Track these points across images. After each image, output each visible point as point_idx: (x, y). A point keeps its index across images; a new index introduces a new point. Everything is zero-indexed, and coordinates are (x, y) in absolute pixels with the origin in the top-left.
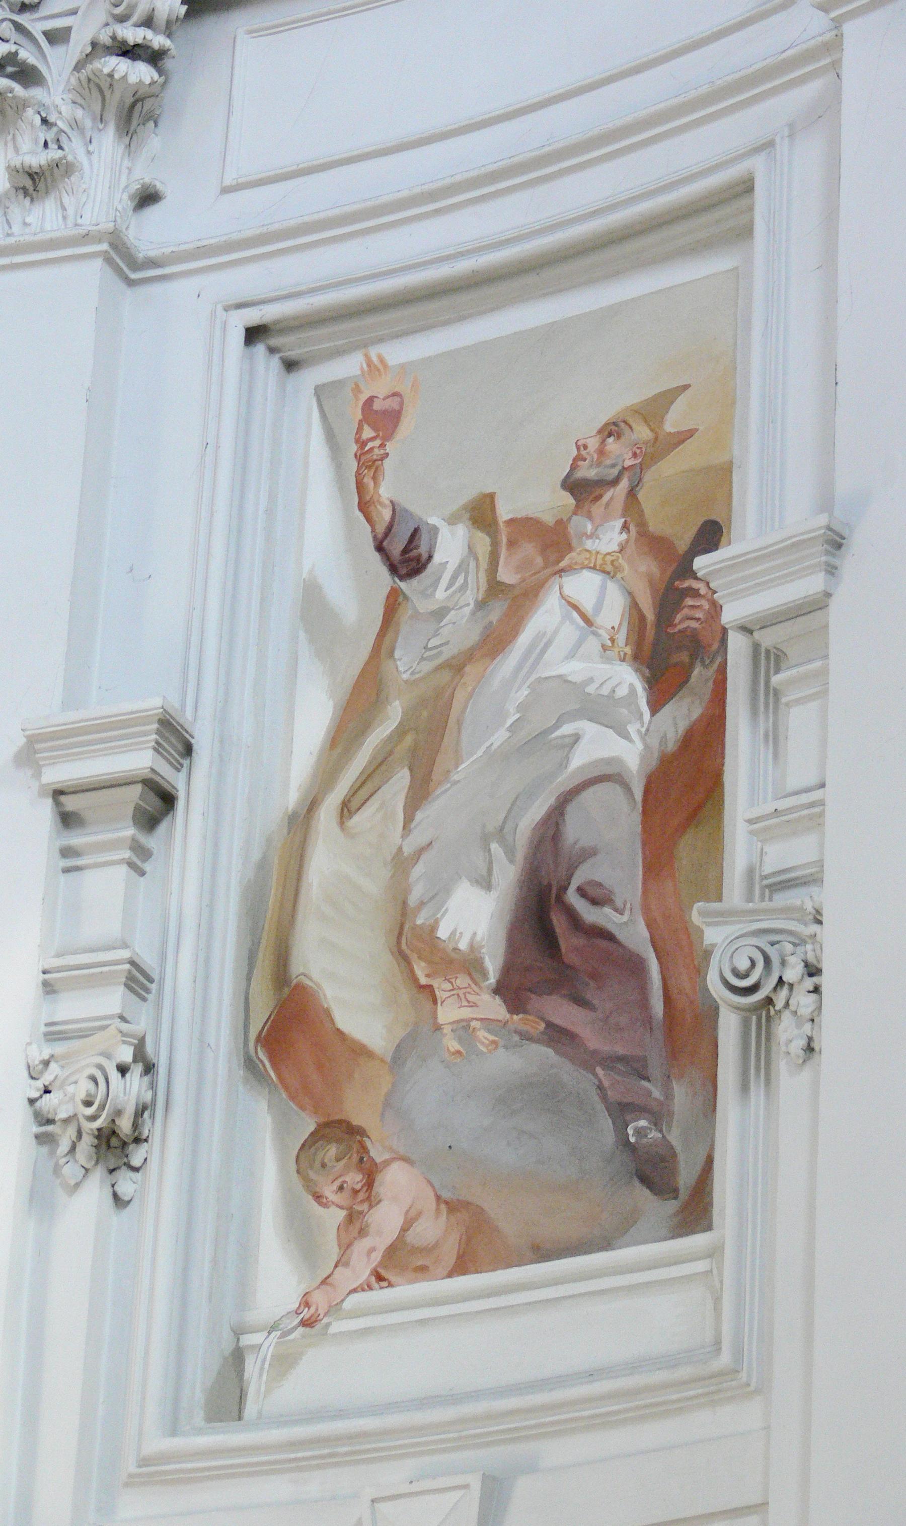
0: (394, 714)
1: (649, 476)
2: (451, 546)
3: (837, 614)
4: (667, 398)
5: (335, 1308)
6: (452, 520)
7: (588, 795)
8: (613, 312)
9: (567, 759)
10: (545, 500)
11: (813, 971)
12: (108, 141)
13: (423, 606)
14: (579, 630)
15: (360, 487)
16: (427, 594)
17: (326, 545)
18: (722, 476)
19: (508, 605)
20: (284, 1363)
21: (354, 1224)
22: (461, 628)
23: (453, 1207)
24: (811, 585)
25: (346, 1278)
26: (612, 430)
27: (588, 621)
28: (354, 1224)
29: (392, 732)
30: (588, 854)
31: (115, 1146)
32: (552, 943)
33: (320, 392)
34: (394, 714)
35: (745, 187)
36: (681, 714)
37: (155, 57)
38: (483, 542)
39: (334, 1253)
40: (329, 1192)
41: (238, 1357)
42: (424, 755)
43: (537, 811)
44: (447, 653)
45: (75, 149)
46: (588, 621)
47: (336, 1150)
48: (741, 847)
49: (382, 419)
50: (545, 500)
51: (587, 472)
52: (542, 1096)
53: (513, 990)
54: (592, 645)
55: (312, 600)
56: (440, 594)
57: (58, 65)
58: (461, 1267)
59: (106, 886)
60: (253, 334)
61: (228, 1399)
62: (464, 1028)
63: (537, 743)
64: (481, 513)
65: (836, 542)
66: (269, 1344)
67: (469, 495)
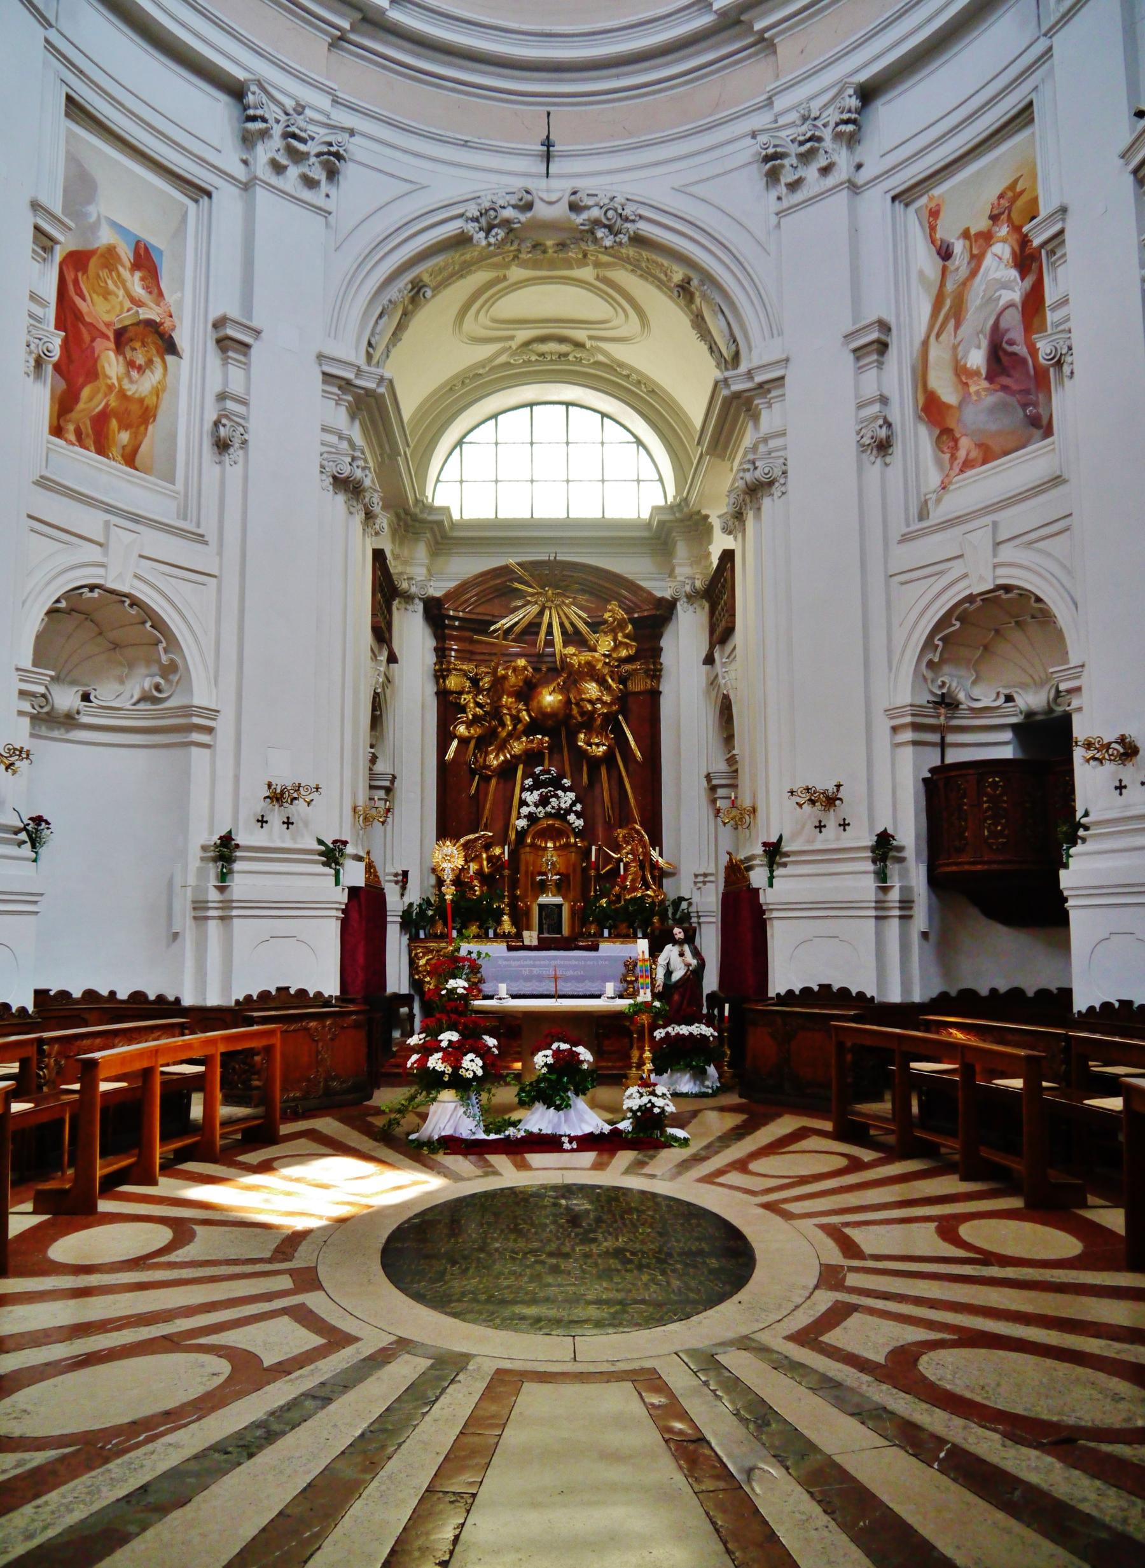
0: (948, 303)
2: (959, 247)
3: (1067, 235)
4: (1016, 181)
5: (950, 483)
6: (958, 239)
7: (1007, 311)
8: (997, 159)
10: (981, 224)
11: (1070, 348)
12: (844, 151)
13: (952, 268)
14: (998, 265)
16: (953, 264)
17: (924, 259)
18: (1035, 201)
19: (976, 260)
20: (939, 501)
21: (953, 457)
22: (964, 271)
23: (980, 445)
25: (953, 473)
26: (1001, 196)
27: (1000, 259)
28: (953, 457)
29: (949, 308)
30: (1007, 330)
31: (883, 447)
32: (1001, 361)
34: (948, 303)
35: (1031, 104)
38: (967, 242)
39: (948, 466)
40: (945, 449)
41: (926, 501)
42: (958, 313)
43: (991, 322)
45: (835, 158)
46: (1000, 259)
47: (946, 436)
48: (1051, 317)
49: (934, 214)
50: (983, 224)
51: (996, 212)
52: (1003, 407)
53: (990, 378)
54: (1002, 266)
55: (921, 273)
57: (827, 134)
58: (984, 462)
60: (894, 199)
61: (923, 515)
62: (977, 393)
63: (990, 300)
64: (966, 234)
65: (1063, 210)
66: (934, 496)
67: (961, 231)
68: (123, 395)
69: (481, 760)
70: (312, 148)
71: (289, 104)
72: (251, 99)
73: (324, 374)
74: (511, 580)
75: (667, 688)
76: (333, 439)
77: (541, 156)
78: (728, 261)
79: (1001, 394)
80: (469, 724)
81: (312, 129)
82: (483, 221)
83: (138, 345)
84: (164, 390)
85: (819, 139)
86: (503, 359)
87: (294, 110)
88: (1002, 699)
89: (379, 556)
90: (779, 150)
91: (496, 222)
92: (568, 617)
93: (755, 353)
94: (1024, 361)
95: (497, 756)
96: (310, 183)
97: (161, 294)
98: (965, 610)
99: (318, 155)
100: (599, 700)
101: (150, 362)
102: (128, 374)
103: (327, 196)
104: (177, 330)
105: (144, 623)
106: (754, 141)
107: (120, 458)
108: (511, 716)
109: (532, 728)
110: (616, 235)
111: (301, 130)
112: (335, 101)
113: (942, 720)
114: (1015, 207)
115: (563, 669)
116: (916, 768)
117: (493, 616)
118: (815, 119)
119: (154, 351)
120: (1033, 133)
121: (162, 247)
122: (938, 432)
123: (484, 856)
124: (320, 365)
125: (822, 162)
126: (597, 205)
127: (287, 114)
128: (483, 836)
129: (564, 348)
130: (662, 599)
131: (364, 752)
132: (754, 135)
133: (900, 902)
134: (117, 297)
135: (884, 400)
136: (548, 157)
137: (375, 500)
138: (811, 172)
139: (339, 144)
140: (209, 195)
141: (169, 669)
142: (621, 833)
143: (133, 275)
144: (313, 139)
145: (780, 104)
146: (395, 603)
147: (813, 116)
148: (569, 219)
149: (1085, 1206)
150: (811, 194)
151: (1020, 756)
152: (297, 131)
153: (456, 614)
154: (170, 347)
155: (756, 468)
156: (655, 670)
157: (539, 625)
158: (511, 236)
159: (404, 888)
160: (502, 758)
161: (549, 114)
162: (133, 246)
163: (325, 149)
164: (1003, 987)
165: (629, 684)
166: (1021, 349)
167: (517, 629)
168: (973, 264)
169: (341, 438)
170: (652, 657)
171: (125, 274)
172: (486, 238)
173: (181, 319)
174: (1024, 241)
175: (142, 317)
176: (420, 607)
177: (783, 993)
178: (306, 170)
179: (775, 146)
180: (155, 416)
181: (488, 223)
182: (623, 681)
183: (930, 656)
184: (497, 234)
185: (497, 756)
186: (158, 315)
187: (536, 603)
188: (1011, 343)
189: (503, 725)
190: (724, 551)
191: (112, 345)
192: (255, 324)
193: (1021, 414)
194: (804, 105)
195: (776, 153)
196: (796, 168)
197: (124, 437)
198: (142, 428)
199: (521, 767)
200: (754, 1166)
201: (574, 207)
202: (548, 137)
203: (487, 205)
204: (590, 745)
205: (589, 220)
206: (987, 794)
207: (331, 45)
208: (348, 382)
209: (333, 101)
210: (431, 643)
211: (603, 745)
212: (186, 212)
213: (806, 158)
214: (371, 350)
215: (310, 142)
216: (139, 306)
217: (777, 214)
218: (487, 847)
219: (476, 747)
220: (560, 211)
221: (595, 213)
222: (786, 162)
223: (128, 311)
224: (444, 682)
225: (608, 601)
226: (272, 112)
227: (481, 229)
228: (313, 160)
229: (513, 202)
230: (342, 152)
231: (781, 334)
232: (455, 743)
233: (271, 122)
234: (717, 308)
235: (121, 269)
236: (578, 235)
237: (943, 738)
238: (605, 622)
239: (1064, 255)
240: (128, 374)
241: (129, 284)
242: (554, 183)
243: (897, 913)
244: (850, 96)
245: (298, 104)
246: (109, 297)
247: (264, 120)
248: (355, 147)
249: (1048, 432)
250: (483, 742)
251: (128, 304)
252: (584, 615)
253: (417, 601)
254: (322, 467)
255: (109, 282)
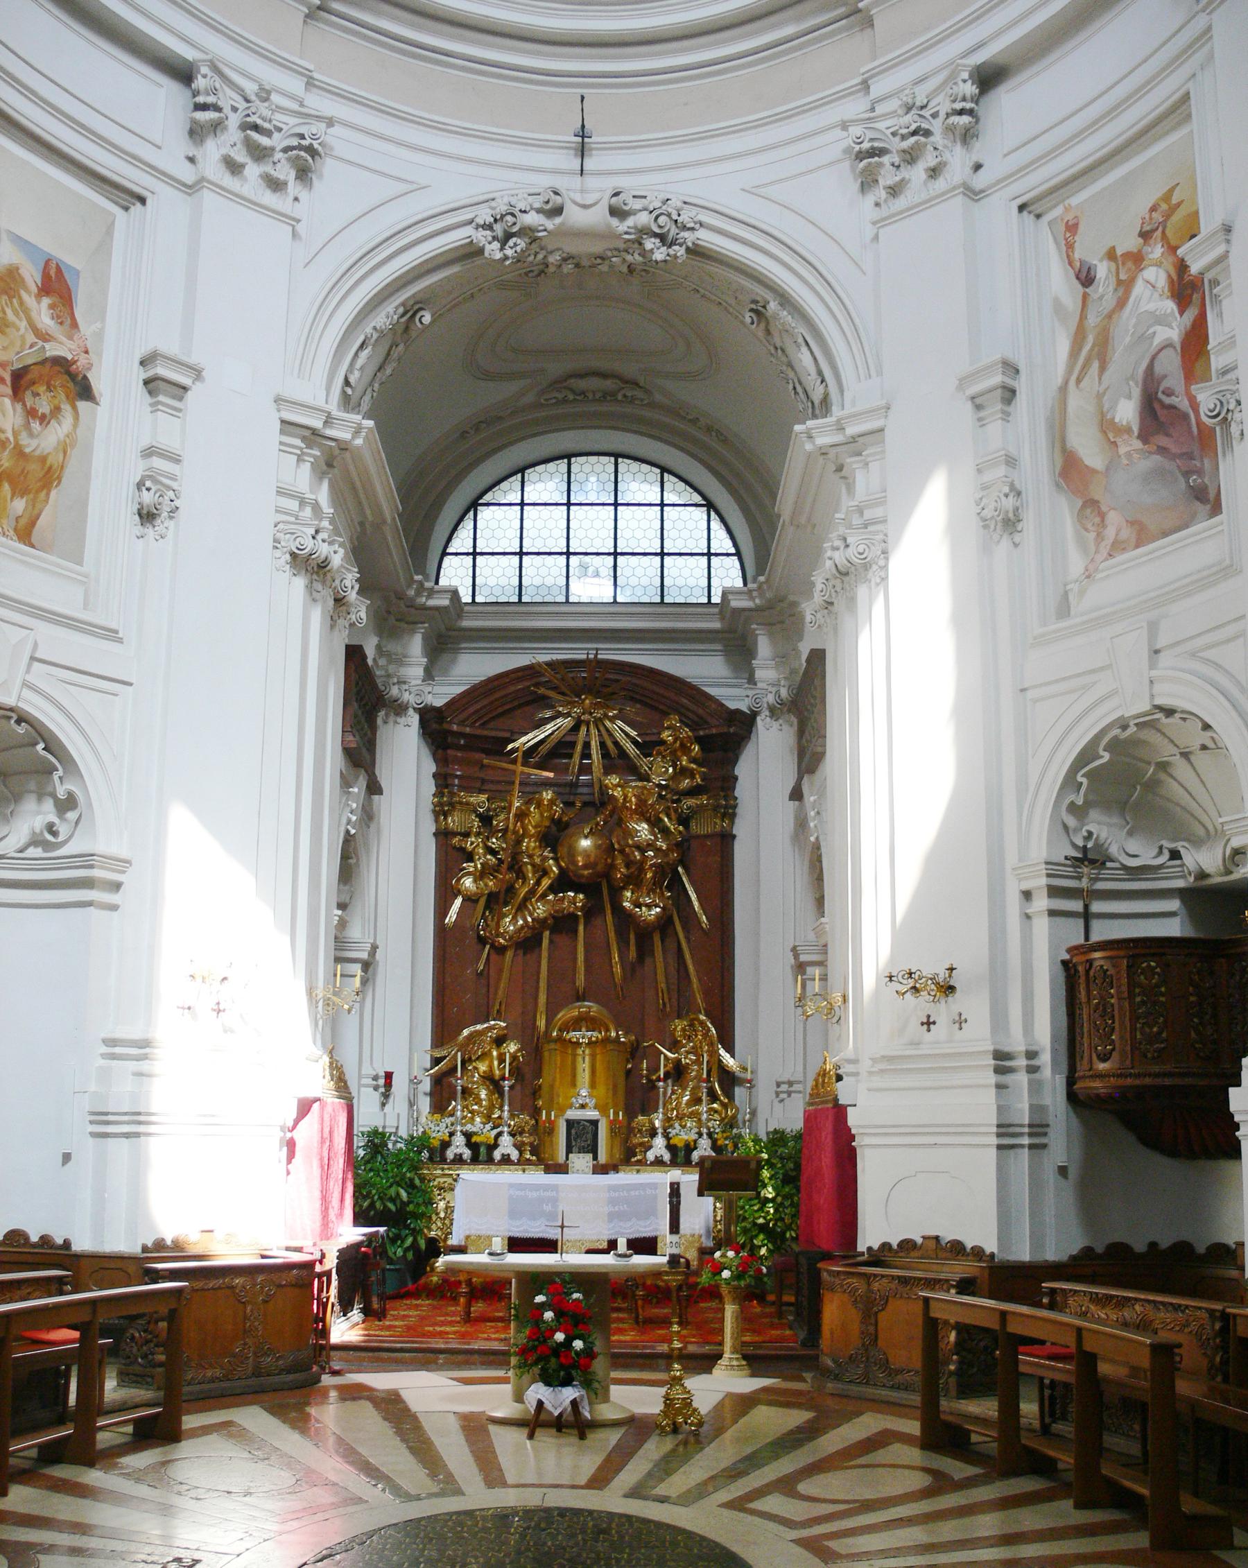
0: (1090, 339)
1: (1169, 224)
2: (1103, 271)
3: (1232, 259)
4: (1171, 191)
5: (1096, 570)
6: (1101, 260)
7: (1162, 354)
9: (1151, 344)
10: (1129, 242)
11: (1239, 403)
12: (958, 148)
14: (1151, 292)
15: (1068, 256)
16: (1096, 291)
19: (1125, 286)
20: (1082, 593)
21: (1100, 537)
22: (1109, 301)
23: (1132, 523)
24: (1220, 249)
25: (1099, 558)
26: (1153, 209)
28: (1100, 537)
29: (1091, 347)
30: (1165, 376)
31: (1011, 523)
32: (1158, 415)
33: (1050, 223)
34: (1090, 339)
35: (1186, 98)
36: (1191, 314)
37: (971, 112)
38: (1113, 265)
39: (1093, 548)
40: (1089, 526)
41: (1066, 595)
42: (1102, 354)
44: (1106, 312)
45: (947, 156)
47: (1090, 509)
48: (1217, 362)
49: (1072, 228)
50: (1129, 242)
51: (1148, 228)
53: (1144, 436)
54: (1156, 295)
56: (1101, 290)
58: (1137, 546)
59: (995, 428)
61: (1064, 610)
62: (1128, 454)
63: (1142, 338)
64: (1111, 255)
65: (1228, 229)
67: (1104, 250)
68: (20, 453)
69: (493, 924)
70: (277, 141)
71: (250, 88)
72: (200, 83)
73: (283, 422)
74: (537, 685)
75: (741, 829)
76: (293, 505)
77: (576, 149)
78: (811, 280)
79: (1158, 458)
80: (480, 876)
81: (279, 118)
82: (499, 228)
83: (42, 389)
84: (73, 446)
85: (927, 133)
86: (530, 398)
87: (257, 95)
88: (1166, 855)
89: (354, 654)
90: (876, 144)
91: (515, 229)
92: (610, 734)
93: (848, 395)
94: (1185, 417)
95: (514, 919)
96: (276, 185)
97: (75, 325)
98: (1116, 738)
99: (286, 150)
100: (650, 846)
101: (57, 410)
102: (27, 426)
103: (296, 199)
104: (94, 369)
105: (36, 744)
106: (845, 134)
107: (12, 533)
108: (533, 865)
109: (564, 882)
110: (670, 246)
111: (264, 119)
112: (310, 83)
113: (1084, 883)
114: (1170, 223)
115: (603, 804)
116: (1053, 947)
117: (513, 733)
118: (922, 108)
119: (63, 396)
120: (1192, 131)
121: (79, 268)
122: (1079, 503)
123: (495, 1053)
124: (279, 411)
125: (929, 160)
126: (645, 209)
127: (247, 101)
128: (491, 1028)
129: (609, 384)
130: (738, 711)
131: (328, 914)
132: (844, 126)
133: (1030, 1126)
134: (18, 330)
135: (1011, 461)
136: (582, 151)
137: (348, 583)
138: (917, 174)
139: (314, 137)
140: (143, 201)
141: (67, 804)
142: (679, 1025)
143: (39, 303)
144: (280, 130)
145: (877, 89)
146: (382, 714)
147: (918, 104)
148: (609, 226)
149: (1231, 1546)
150: (917, 200)
151: (1190, 933)
152: (259, 122)
153: (462, 729)
154: (85, 391)
155: (847, 546)
156: (726, 807)
157: (573, 745)
158: (534, 246)
159: (386, 1096)
160: (521, 922)
161: (583, 98)
162: (42, 265)
163: (294, 142)
164: (1165, 1243)
165: (693, 824)
166: (1182, 402)
167: (543, 750)
168: (1120, 293)
169: (303, 502)
170: (723, 789)
171: (30, 300)
172: (502, 249)
173: (100, 355)
174: (1182, 267)
175: (48, 354)
176: (414, 719)
177: (876, 1247)
178: (268, 168)
179: (872, 140)
180: (59, 479)
181: (505, 231)
182: (684, 821)
183: (1072, 797)
184: (515, 245)
185: (514, 919)
186: (70, 350)
187: (568, 715)
188: (1169, 393)
189: (525, 879)
190: (812, 650)
191: (9, 391)
192: (193, 360)
193: (1183, 485)
194: (907, 92)
195: (873, 148)
196: (898, 167)
197: (19, 505)
198: (43, 493)
199: (547, 934)
200: (802, 1487)
201: (616, 212)
202: (583, 126)
203: (504, 208)
204: (639, 906)
205: (635, 227)
206: (1140, 985)
207: (307, 16)
208: (314, 432)
209: (308, 83)
210: (430, 767)
211: (657, 906)
212: (113, 223)
213: (910, 157)
214: (349, 391)
215: (276, 135)
216: (46, 341)
217: (874, 223)
218: (499, 1041)
219: (488, 906)
220: (597, 217)
221: (643, 219)
222: (886, 159)
223: (31, 346)
224: (445, 819)
225: (665, 714)
226: (227, 98)
227: (494, 238)
228: (278, 155)
229: (537, 205)
230: (316, 146)
231: (880, 373)
232: (458, 902)
233: (227, 110)
234: (800, 340)
235: (23, 293)
236: (622, 246)
237: (1086, 907)
238: (663, 742)
239: (1230, 285)
240: (27, 426)
241: (34, 314)
242: (591, 182)
243: (1026, 1141)
244: (965, 81)
245: (262, 88)
246: (7, 330)
247: (217, 109)
248: (335, 138)
249: (1216, 508)
250: (494, 902)
251: (31, 338)
252: (633, 733)
253: (411, 711)
254: (276, 541)
255: (9, 311)
